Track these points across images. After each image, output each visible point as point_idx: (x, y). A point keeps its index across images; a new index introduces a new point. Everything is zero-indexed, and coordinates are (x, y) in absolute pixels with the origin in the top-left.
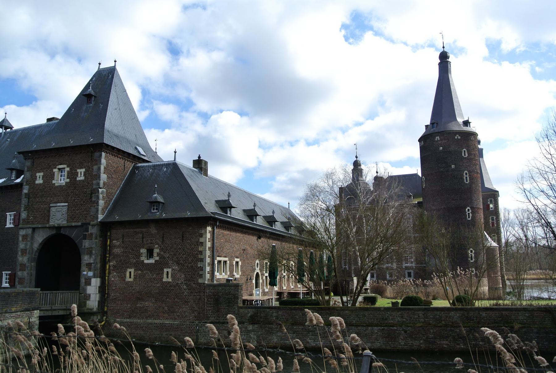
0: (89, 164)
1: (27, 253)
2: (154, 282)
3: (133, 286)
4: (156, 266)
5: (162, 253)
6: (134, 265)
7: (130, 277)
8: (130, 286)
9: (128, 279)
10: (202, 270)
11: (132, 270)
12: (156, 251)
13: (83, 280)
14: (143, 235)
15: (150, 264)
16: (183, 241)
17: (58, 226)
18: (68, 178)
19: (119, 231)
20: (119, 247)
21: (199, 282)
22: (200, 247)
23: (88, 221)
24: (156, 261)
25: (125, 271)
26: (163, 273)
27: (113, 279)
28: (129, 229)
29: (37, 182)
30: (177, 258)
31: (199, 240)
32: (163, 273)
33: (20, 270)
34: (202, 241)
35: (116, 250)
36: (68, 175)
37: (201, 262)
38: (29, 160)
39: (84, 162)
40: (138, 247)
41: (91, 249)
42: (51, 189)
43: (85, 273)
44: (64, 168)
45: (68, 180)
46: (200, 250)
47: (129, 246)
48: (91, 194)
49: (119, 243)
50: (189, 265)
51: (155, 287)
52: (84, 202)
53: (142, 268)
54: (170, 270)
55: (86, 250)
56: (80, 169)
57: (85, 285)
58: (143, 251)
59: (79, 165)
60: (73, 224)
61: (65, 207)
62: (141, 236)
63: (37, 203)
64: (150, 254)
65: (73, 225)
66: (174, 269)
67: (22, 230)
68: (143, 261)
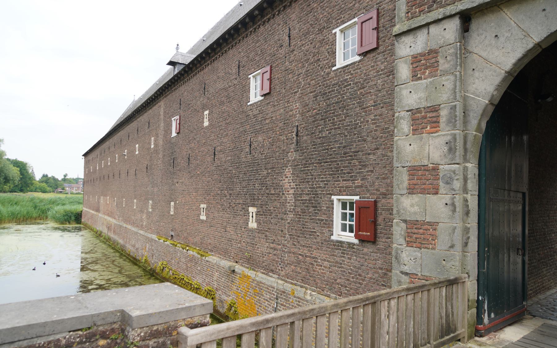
1: (443, 120)
33: (411, 191)
67: (407, 40)
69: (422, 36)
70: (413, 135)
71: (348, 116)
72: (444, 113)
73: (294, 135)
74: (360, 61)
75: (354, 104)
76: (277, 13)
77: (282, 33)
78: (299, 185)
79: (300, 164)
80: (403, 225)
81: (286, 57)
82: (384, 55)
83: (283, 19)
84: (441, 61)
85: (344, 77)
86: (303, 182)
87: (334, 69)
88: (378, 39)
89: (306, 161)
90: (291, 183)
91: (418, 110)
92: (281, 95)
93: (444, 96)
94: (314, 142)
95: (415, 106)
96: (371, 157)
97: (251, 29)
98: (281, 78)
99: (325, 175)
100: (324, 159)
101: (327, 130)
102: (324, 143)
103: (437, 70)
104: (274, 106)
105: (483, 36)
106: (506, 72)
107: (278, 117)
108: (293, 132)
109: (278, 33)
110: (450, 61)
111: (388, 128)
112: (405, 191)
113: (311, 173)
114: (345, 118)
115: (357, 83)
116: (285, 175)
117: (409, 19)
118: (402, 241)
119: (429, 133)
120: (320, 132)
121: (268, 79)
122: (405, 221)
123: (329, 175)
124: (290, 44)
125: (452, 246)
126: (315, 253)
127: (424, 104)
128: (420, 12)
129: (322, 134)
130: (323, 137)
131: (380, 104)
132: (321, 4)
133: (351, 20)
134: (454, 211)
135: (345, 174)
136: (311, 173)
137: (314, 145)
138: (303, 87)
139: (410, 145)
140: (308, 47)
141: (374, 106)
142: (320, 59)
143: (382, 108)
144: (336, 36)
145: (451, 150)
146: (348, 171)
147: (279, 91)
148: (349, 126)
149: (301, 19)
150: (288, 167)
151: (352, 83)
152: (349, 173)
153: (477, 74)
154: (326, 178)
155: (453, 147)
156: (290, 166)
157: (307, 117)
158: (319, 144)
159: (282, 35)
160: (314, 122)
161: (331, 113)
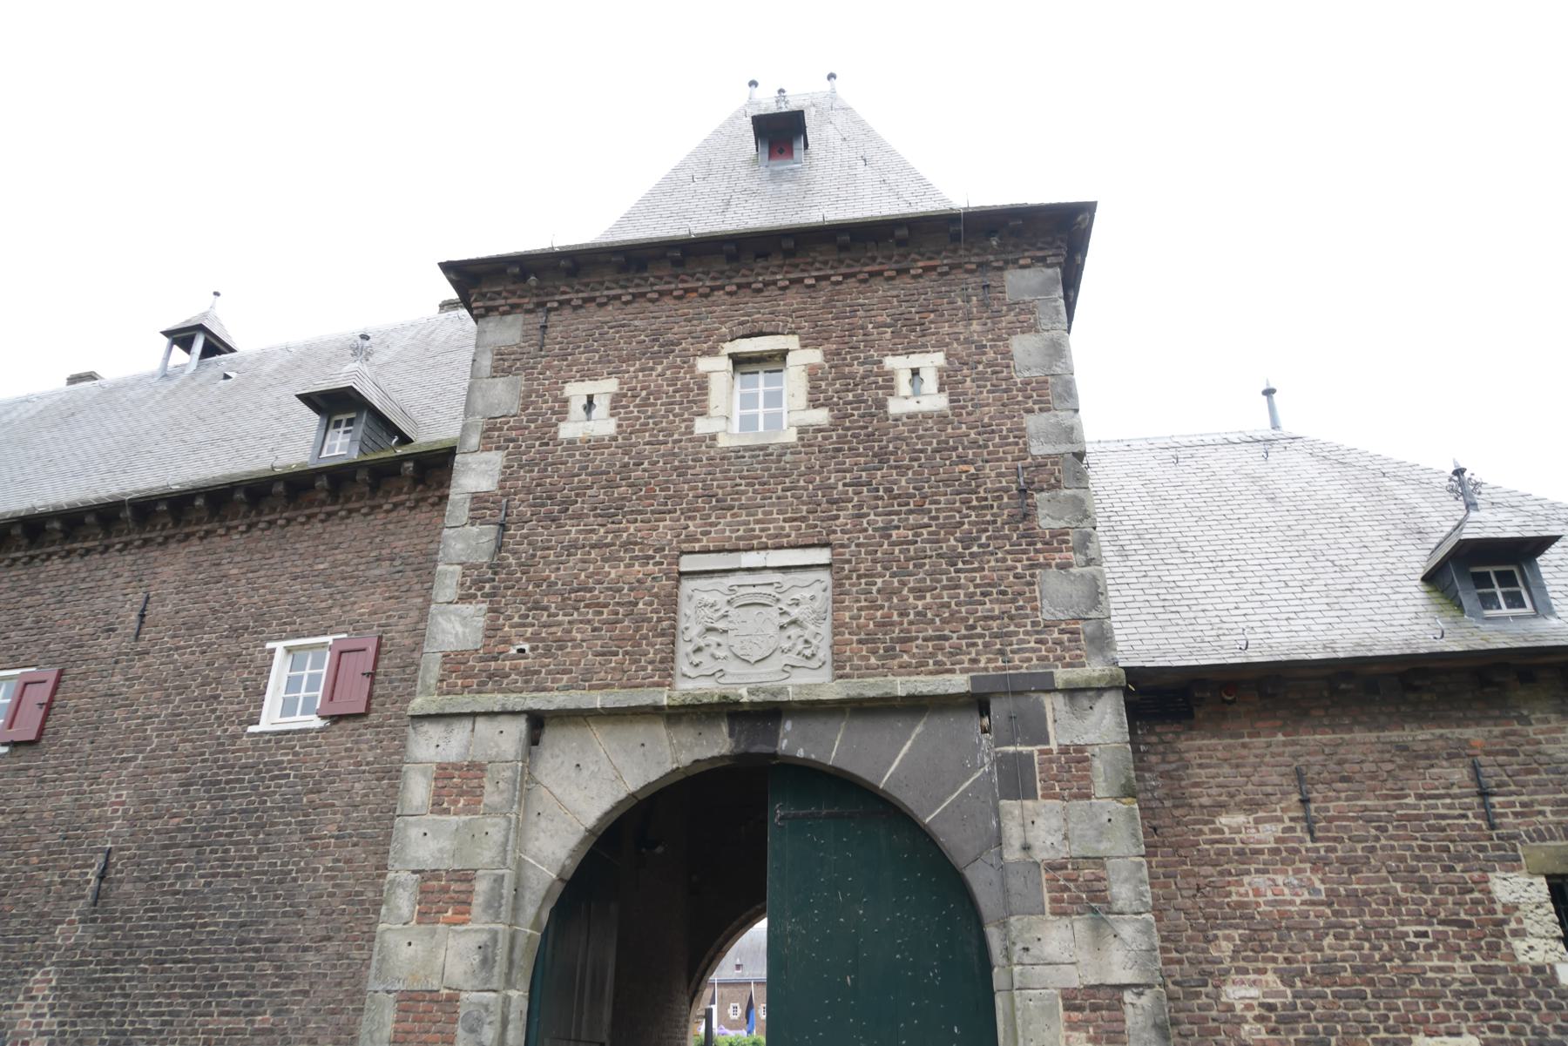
1: (478, 900)
6: (1471, 1007)
14: (1475, 769)
18: (814, 404)
20: (1283, 855)
23: (1024, 663)
35: (1260, 880)
36: (814, 389)
38: (509, 318)
40: (1460, 858)
42: (681, 471)
47: (1372, 850)
49: (1268, 834)
52: (967, 541)
55: (1044, 876)
60: (901, 686)
62: (1460, 774)
67: (433, 731)
69: (461, 731)
70: (419, 923)
71: (267, 850)
72: (482, 886)
73: (92, 875)
74: (321, 730)
75: (289, 824)
76: (118, 546)
77: (121, 598)
78: (74, 1024)
79: (91, 962)
81: (116, 662)
82: (378, 733)
83: (134, 568)
84: (489, 788)
85: (274, 755)
86: (91, 1015)
87: (251, 729)
88: (370, 696)
89: (116, 954)
90: (43, 1015)
91: (435, 874)
92: (76, 755)
93: (485, 855)
94: (154, 902)
96: (310, 957)
97: (18, 554)
98: (87, 710)
99: (168, 996)
100: (174, 952)
101: (201, 876)
102: (185, 909)
103: (480, 802)
104: (43, 781)
105: (560, 760)
106: (587, 830)
107: (45, 815)
108: (92, 866)
109: (108, 594)
110: (503, 792)
111: (362, 893)
114: (260, 851)
115: (304, 776)
116: (29, 990)
117: (441, 694)
119: (450, 924)
120: (178, 877)
121: (41, 705)
123: (183, 996)
124: (138, 634)
128: (464, 687)
129: (184, 884)
130: (186, 893)
131: (351, 836)
132: (250, 575)
133: (316, 636)
135: (230, 995)
136: (123, 988)
137: (153, 910)
138: (153, 751)
139: (410, 944)
140: (192, 657)
141: (337, 838)
142: (219, 696)
143: (355, 845)
144: (272, 658)
145: (487, 962)
146: (242, 988)
147: (70, 744)
148: (265, 873)
149: (186, 586)
150: (43, 965)
151: (292, 773)
152: (241, 995)
153: (543, 823)
154: (170, 1005)
155: (490, 955)
156: (53, 964)
157: (147, 832)
158: (169, 909)
159: (119, 604)
160: (165, 847)
161: (221, 835)
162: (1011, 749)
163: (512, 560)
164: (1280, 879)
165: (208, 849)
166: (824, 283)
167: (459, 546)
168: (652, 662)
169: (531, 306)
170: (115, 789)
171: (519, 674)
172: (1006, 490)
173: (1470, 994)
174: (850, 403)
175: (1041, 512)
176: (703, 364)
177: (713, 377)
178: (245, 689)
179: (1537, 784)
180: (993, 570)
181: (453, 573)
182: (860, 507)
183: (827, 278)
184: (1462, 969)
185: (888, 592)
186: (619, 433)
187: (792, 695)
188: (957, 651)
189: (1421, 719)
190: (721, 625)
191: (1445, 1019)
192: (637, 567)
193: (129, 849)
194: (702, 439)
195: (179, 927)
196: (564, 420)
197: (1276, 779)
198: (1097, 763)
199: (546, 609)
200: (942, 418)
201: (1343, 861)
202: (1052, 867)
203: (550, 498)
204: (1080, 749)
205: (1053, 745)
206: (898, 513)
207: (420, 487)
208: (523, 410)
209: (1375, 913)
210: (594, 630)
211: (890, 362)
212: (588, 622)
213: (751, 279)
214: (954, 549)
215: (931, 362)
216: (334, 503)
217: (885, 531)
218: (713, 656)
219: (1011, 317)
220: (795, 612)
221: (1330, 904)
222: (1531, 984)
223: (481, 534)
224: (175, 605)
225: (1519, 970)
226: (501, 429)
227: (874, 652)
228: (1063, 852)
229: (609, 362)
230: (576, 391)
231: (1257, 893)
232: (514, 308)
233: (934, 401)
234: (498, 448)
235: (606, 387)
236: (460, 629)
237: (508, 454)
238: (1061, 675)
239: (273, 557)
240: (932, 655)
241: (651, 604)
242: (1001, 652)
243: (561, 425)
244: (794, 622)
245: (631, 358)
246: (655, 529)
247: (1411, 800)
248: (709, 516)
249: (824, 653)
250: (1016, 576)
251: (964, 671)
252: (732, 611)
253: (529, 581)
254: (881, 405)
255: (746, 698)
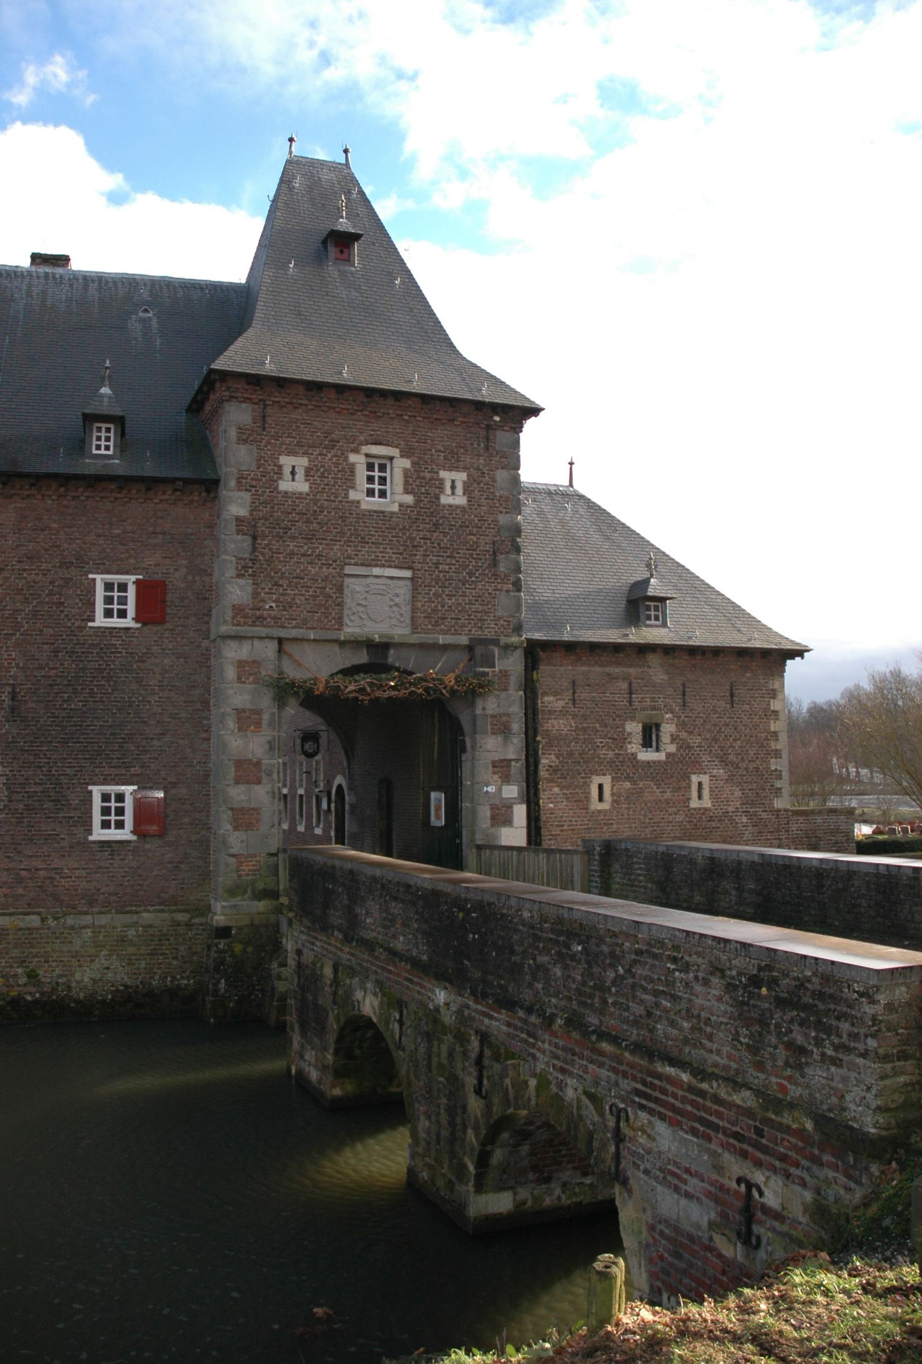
0: (481, 461)
1: (265, 723)
2: (667, 811)
3: (612, 824)
4: (671, 769)
5: (684, 735)
6: (611, 766)
7: (601, 799)
8: (605, 824)
9: (595, 805)
10: (781, 779)
11: (607, 781)
12: (668, 729)
13: (485, 812)
14: (630, 684)
15: (654, 762)
16: (733, 707)
17: (383, 640)
19: (563, 668)
20: (563, 713)
21: (775, 806)
22: (772, 722)
23: (488, 634)
24: (668, 755)
25: (585, 783)
26: (689, 786)
27: (551, 805)
28: (589, 665)
29: (285, 485)
30: (722, 748)
31: (769, 705)
32: (690, 788)
33: (237, 782)
34: (776, 709)
35: (554, 722)
36: (406, 483)
37: (776, 758)
38: (243, 405)
39: (462, 451)
40: (618, 716)
41: (504, 718)
43: (491, 789)
44: (391, 459)
45: (409, 499)
46: (772, 729)
47: (592, 712)
48: (495, 554)
49: (561, 704)
50: (751, 766)
51: (671, 822)
52: (471, 574)
53: (634, 773)
54: (705, 779)
55: (489, 720)
56: (451, 470)
57: (492, 825)
58: (634, 728)
59: (445, 458)
60: (442, 640)
61: (402, 583)
62: (625, 686)
63: (292, 554)
64: (649, 736)
65: (441, 642)
66: (714, 776)
67: (233, 644)
68: (634, 755)
70: (239, 731)
72: (266, 717)
74: (137, 629)
75: (127, 677)
78: (20, 771)
80: (230, 813)
86: (30, 767)
87: (90, 624)
91: (244, 711)
95: (240, 706)
96: (155, 742)
112: (232, 782)
113: (45, 755)
114: (113, 690)
115: (132, 653)
117: (234, 625)
118: (229, 827)
120: (64, 701)
122: (232, 809)
123: (84, 759)
125: (273, 826)
126: (57, 863)
127: (249, 706)
130: (71, 709)
132: (67, 530)
134: (274, 797)
135: (113, 759)
143: (170, 690)
144: (95, 584)
145: (271, 748)
152: (119, 758)
162: (481, 669)
163: (261, 557)
164: (561, 721)
165: (80, 688)
166: (412, 419)
167: (233, 546)
168: (334, 618)
169: (257, 401)
170: (6, 651)
171: (271, 618)
172: (488, 551)
173: (611, 762)
174: (423, 493)
175: (501, 565)
176: (353, 458)
177: (358, 466)
178: (81, 600)
179: (648, 691)
180: (480, 589)
181: (231, 561)
182: (426, 551)
183: (415, 417)
184: (611, 754)
185: (436, 595)
186: (311, 492)
187: (397, 640)
188: (464, 626)
189: (618, 664)
190: (363, 602)
191: (602, 770)
192: (324, 569)
193: (26, 685)
194: (353, 502)
195: (71, 726)
196: (280, 478)
197: (565, 684)
198: (512, 678)
199: (281, 586)
200: (463, 509)
201: (582, 716)
202: (493, 716)
203: (278, 524)
204: (506, 672)
205: (497, 669)
206: (442, 556)
207: (179, 493)
208: (258, 468)
209: (589, 735)
210: (306, 599)
211: (443, 474)
212: (303, 595)
213: (377, 410)
214: (465, 577)
215: (461, 477)
216: (120, 492)
217: (437, 564)
218: (360, 618)
219: (497, 458)
220: (397, 600)
221: (575, 731)
222: (629, 759)
223: (243, 540)
224: (14, 541)
225: (627, 755)
226: (246, 478)
227: (430, 622)
228: (497, 711)
229: (303, 446)
230: (287, 461)
231: (553, 726)
232: (245, 400)
233: (460, 500)
234: (246, 490)
235: (302, 462)
236: (239, 593)
237: (253, 495)
238: (503, 640)
239: (80, 520)
240: (453, 626)
241: (331, 589)
242: (480, 628)
243: (280, 482)
244: (396, 605)
245: (313, 446)
246: (332, 549)
247: (608, 695)
248: (357, 546)
249: (408, 621)
250: (490, 594)
251: (465, 635)
252: (368, 596)
253: (272, 569)
254: (438, 498)
255: (377, 640)
